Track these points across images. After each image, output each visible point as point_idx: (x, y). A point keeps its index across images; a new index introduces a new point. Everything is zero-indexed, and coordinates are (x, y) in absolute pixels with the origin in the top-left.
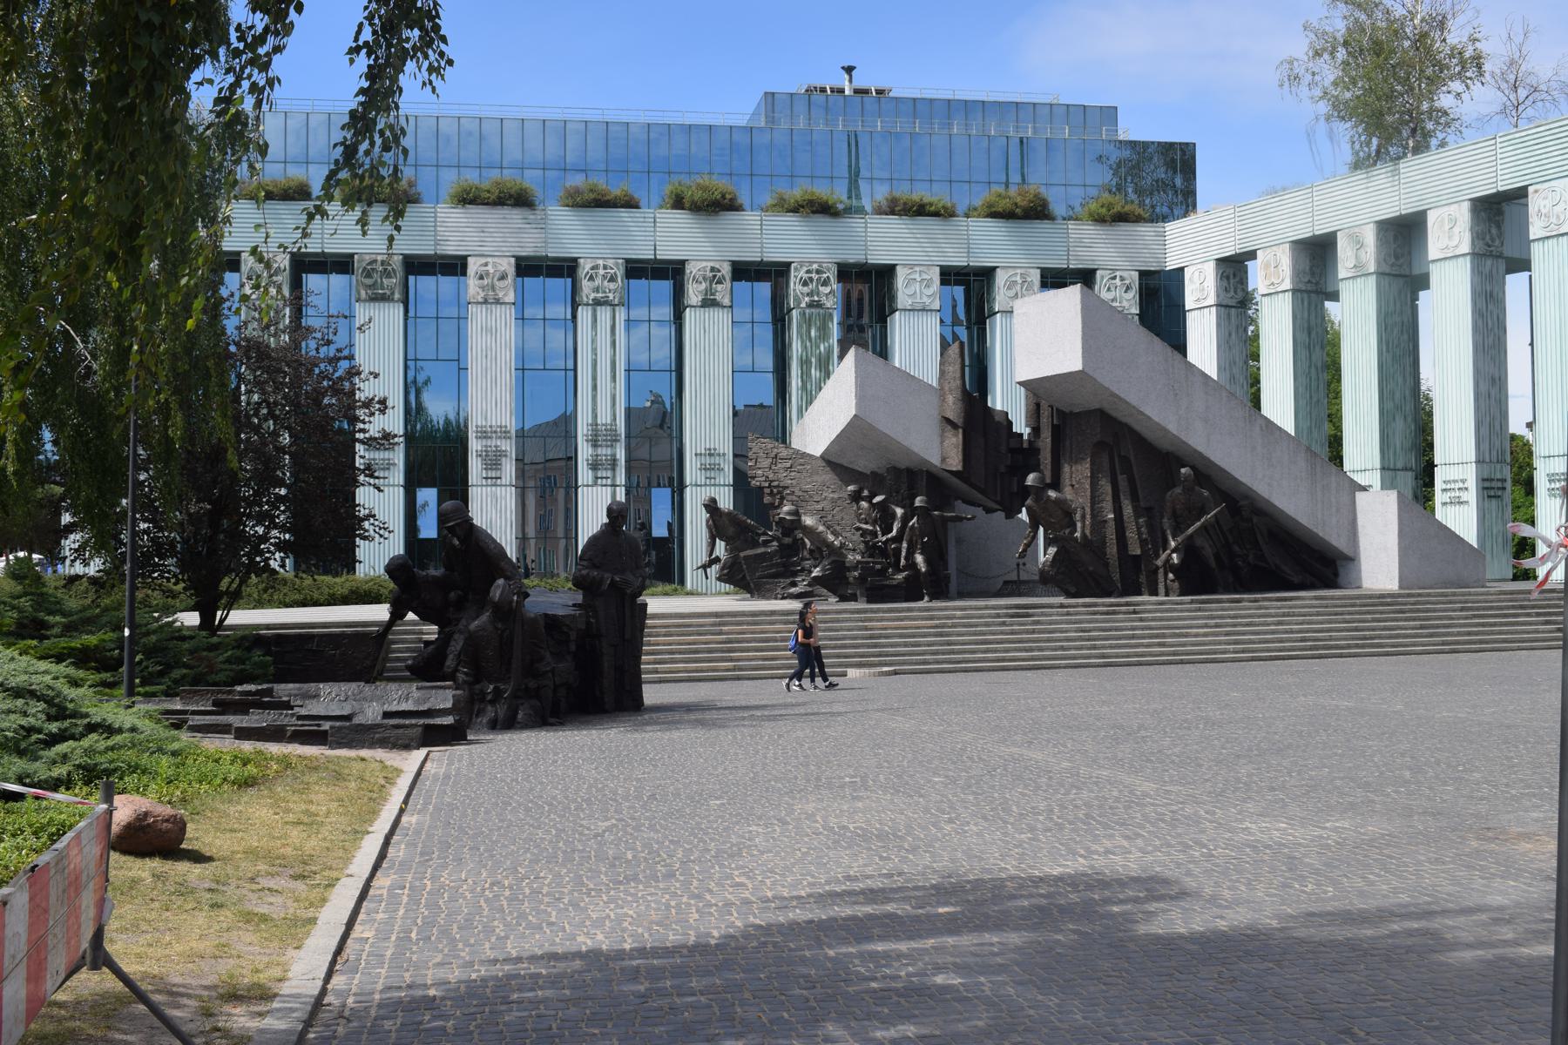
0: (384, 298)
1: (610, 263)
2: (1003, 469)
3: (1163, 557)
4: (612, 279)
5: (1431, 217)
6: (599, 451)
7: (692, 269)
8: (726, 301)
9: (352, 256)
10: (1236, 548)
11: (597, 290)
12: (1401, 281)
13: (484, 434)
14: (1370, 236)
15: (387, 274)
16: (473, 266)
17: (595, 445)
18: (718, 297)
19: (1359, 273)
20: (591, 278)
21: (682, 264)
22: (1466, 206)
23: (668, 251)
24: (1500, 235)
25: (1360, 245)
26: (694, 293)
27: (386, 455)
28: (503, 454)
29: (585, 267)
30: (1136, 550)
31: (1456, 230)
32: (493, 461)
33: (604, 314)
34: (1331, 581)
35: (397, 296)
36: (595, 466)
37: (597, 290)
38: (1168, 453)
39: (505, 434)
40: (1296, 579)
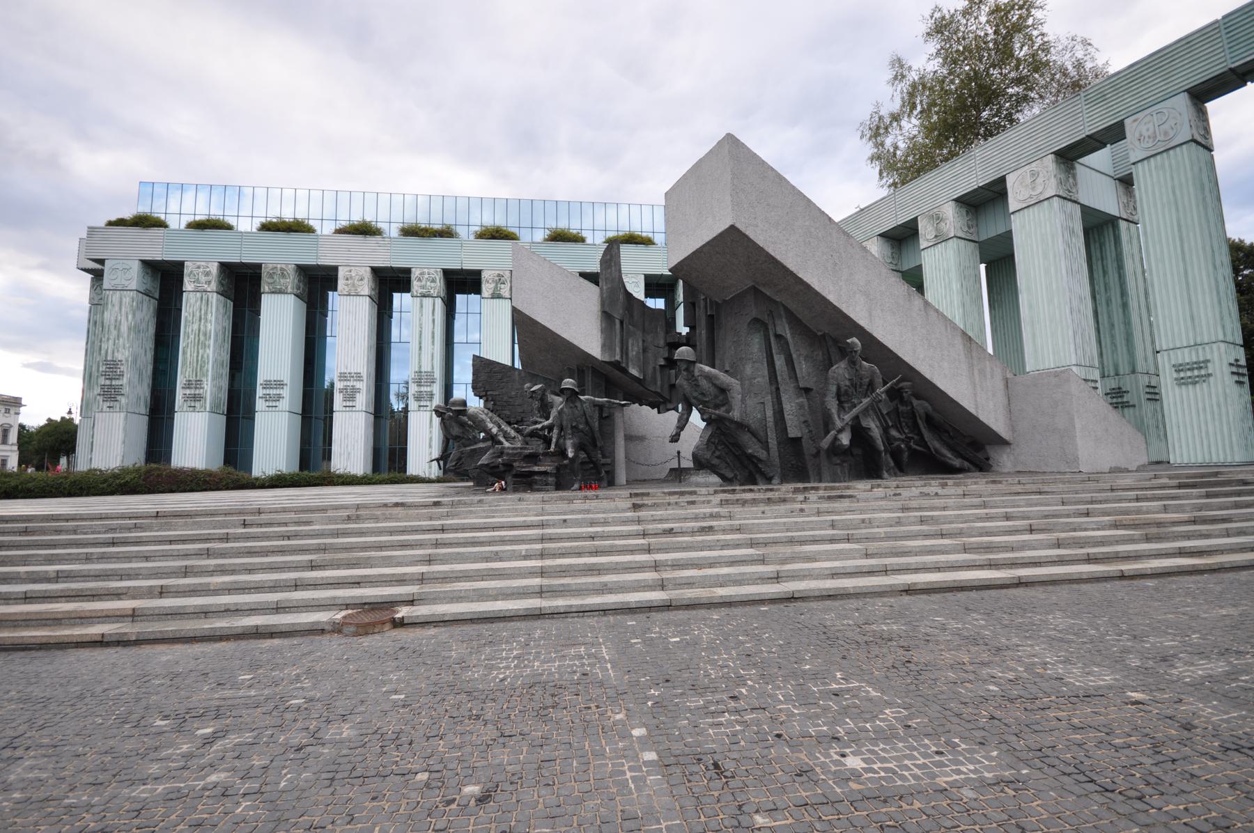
0: (280, 292)
1: (432, 271)
2: (662, 362)
3: (829, 437)
4: (433, 281)
5: (1010, 181)
6: (422, 389)
7: (485, 275)
8: (507, 295)
9: (259, 266)
10: (894, 433)
11: (422, 287)
12: (972, 244)
13: (343, 377)
14: (949, 211)
15: (283, 275)
16: (342, 273)
17: (419, 384)
18: (502, 292)
19: (941, 239)
20: (419, 280)
21: (478, 273)
22: (1050, 161)
23: (469, 265)
24: (1075, 185)
25: (937, 219)
26: (487, 289)
27: (278, 392)
28: (359, 391)
29: (415, 274)
30: (793, 432)
31: (1040, 180)
32: (350, 395)
33: (428, 302)
34: (981, 465)
35: (289, 290)
36: (418, 398)
37: (422, 287)
38: (824, 336)
39: (358, 377)
40: (957, 462)
